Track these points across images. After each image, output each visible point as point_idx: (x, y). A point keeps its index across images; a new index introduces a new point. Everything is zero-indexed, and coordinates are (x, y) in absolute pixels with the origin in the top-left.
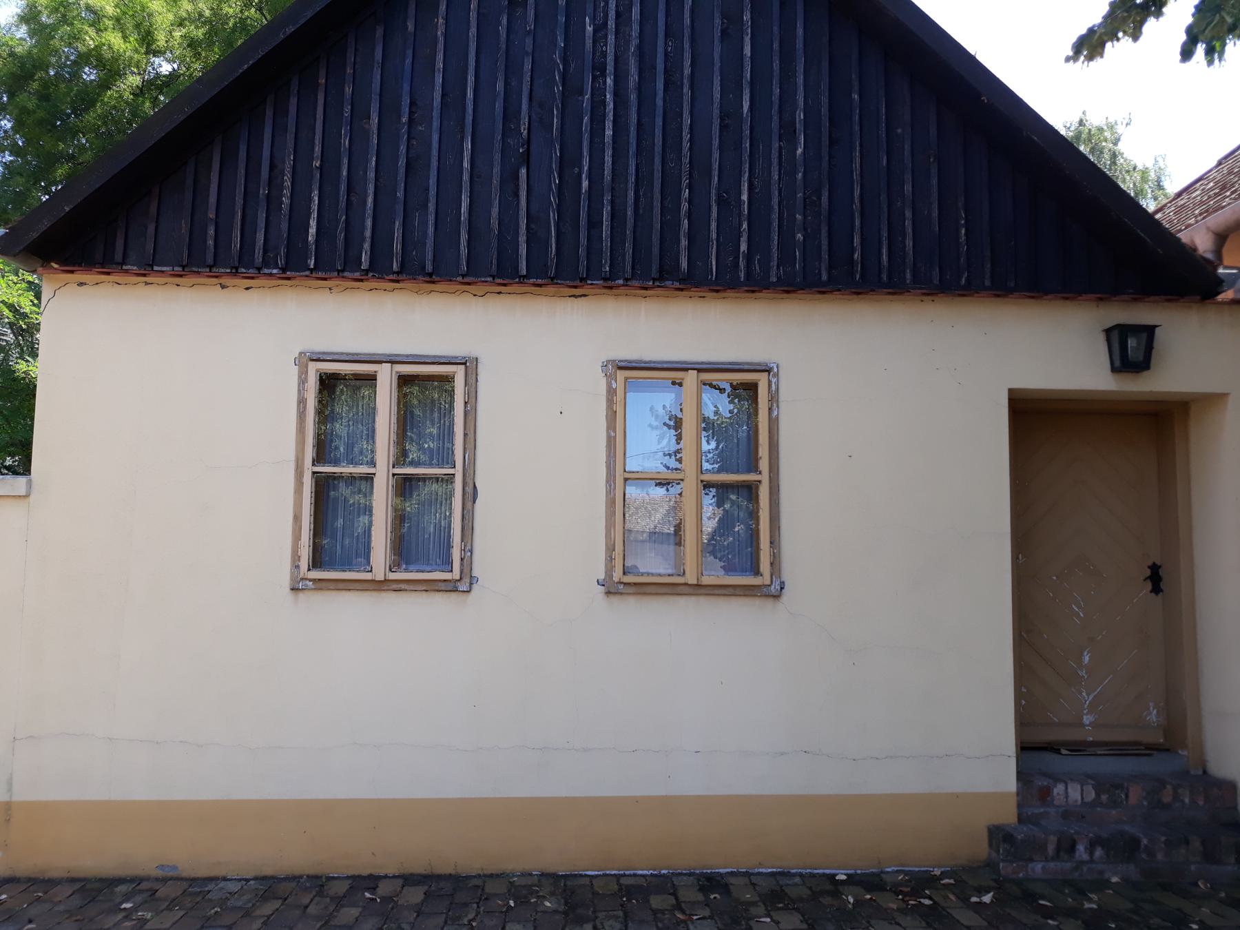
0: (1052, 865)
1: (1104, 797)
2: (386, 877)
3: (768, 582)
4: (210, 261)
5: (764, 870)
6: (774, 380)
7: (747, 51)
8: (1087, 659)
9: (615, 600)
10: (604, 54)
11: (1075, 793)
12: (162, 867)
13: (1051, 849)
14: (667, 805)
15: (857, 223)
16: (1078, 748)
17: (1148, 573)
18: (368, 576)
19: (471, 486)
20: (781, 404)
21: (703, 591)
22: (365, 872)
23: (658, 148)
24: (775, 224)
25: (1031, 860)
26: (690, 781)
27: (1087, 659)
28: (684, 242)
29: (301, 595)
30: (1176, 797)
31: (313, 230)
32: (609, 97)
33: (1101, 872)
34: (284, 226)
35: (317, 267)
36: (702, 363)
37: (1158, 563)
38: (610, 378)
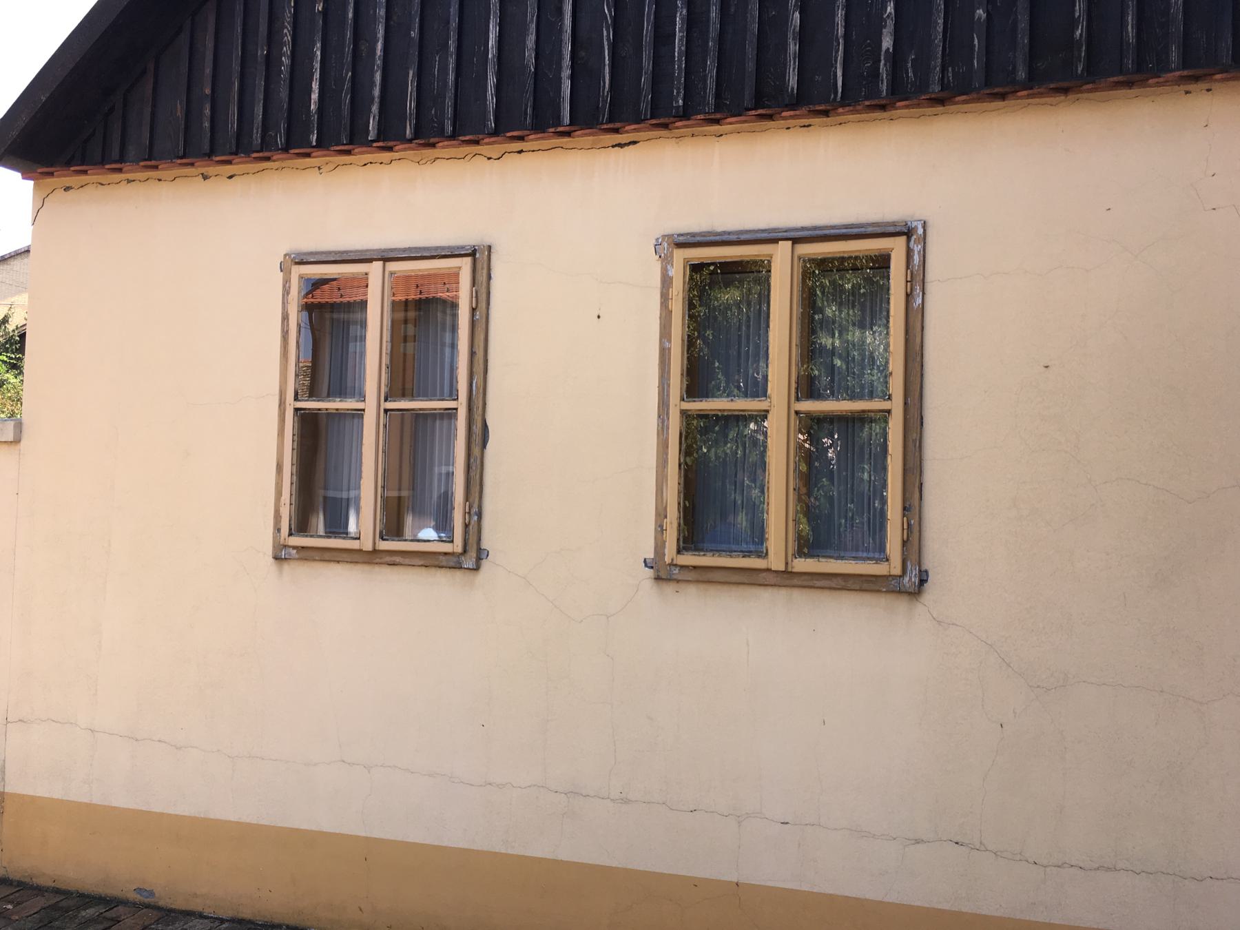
3: (897, 570)
4: (206, 148)
6: (917, 248)
9: (669, 588)
12: (139, 890)
18: (354, 545)
20: (929, 287)
21: (795, 581)
28: (793, 47)
29: (286, 567)
31: (315, 96)
34: (284, 94)
36: (803, 229)
38: (666, 261)
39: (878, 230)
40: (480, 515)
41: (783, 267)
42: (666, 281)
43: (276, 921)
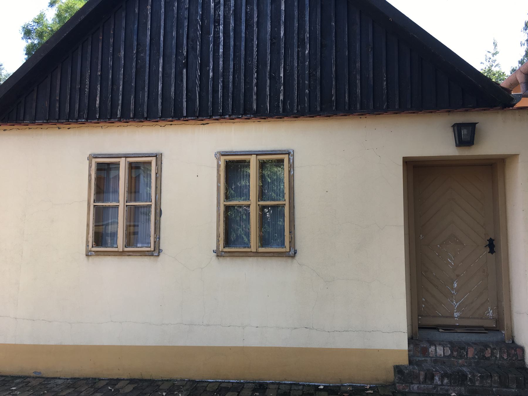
0: (422, 386)
1: (455, 354)
2: (124, 380)
3: (288, 250)
4: (57, 117)
5: (287, 382)
6: (291, 158)
7: (283, 7)
8: (456, 285)
9: (221, 259)
10: (219, 15)
11: (440, 351)
12: (35, 372)
13: (422, 378)
14: (243, 350)
15: (334, 83)
16: (449, 328)
17: (488, 243)
18: (116, 250)
19: (159, 210)
20: (295, 169)
22: (116, 377)
23: (243, 56)
24: (296, 86)
25: (412, 383)
26: (254, 341)
28: (255, 97)
29: (90, 258)
30: (492, 354)
31: (98, 102)
32: (221, 35)
33: (447, 390)
34: (86, 101)
35: (100, 118)
36: (259, 151)
37: (493, 238)
38: (218, 160)
39: (281, 152)
40: (159, 238)
41: (253, 161)
42: (219, 166)
43: (88, 377)
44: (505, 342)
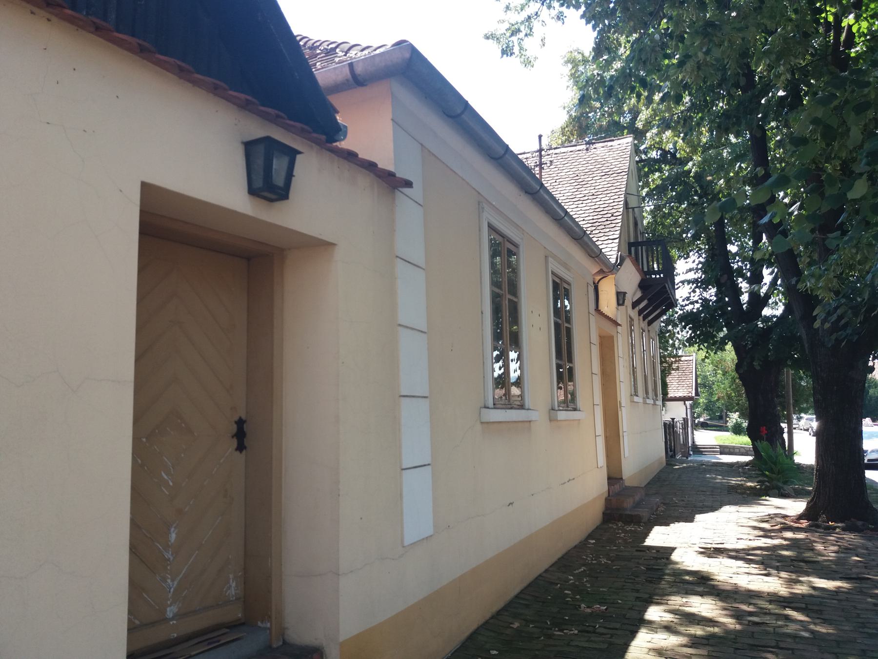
17: (234, 428)
27: (173, 536)
37: (244, 417)
44: (270, 647)
